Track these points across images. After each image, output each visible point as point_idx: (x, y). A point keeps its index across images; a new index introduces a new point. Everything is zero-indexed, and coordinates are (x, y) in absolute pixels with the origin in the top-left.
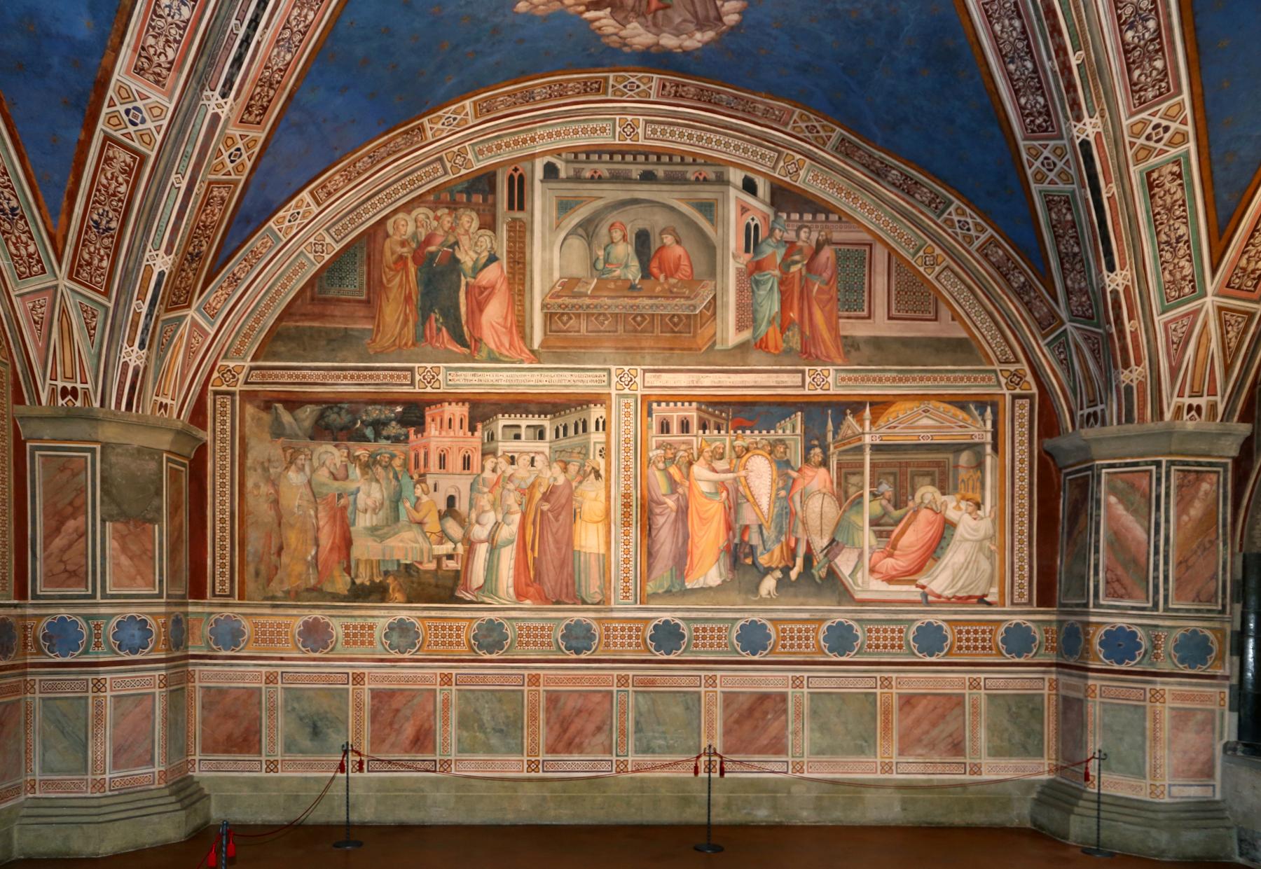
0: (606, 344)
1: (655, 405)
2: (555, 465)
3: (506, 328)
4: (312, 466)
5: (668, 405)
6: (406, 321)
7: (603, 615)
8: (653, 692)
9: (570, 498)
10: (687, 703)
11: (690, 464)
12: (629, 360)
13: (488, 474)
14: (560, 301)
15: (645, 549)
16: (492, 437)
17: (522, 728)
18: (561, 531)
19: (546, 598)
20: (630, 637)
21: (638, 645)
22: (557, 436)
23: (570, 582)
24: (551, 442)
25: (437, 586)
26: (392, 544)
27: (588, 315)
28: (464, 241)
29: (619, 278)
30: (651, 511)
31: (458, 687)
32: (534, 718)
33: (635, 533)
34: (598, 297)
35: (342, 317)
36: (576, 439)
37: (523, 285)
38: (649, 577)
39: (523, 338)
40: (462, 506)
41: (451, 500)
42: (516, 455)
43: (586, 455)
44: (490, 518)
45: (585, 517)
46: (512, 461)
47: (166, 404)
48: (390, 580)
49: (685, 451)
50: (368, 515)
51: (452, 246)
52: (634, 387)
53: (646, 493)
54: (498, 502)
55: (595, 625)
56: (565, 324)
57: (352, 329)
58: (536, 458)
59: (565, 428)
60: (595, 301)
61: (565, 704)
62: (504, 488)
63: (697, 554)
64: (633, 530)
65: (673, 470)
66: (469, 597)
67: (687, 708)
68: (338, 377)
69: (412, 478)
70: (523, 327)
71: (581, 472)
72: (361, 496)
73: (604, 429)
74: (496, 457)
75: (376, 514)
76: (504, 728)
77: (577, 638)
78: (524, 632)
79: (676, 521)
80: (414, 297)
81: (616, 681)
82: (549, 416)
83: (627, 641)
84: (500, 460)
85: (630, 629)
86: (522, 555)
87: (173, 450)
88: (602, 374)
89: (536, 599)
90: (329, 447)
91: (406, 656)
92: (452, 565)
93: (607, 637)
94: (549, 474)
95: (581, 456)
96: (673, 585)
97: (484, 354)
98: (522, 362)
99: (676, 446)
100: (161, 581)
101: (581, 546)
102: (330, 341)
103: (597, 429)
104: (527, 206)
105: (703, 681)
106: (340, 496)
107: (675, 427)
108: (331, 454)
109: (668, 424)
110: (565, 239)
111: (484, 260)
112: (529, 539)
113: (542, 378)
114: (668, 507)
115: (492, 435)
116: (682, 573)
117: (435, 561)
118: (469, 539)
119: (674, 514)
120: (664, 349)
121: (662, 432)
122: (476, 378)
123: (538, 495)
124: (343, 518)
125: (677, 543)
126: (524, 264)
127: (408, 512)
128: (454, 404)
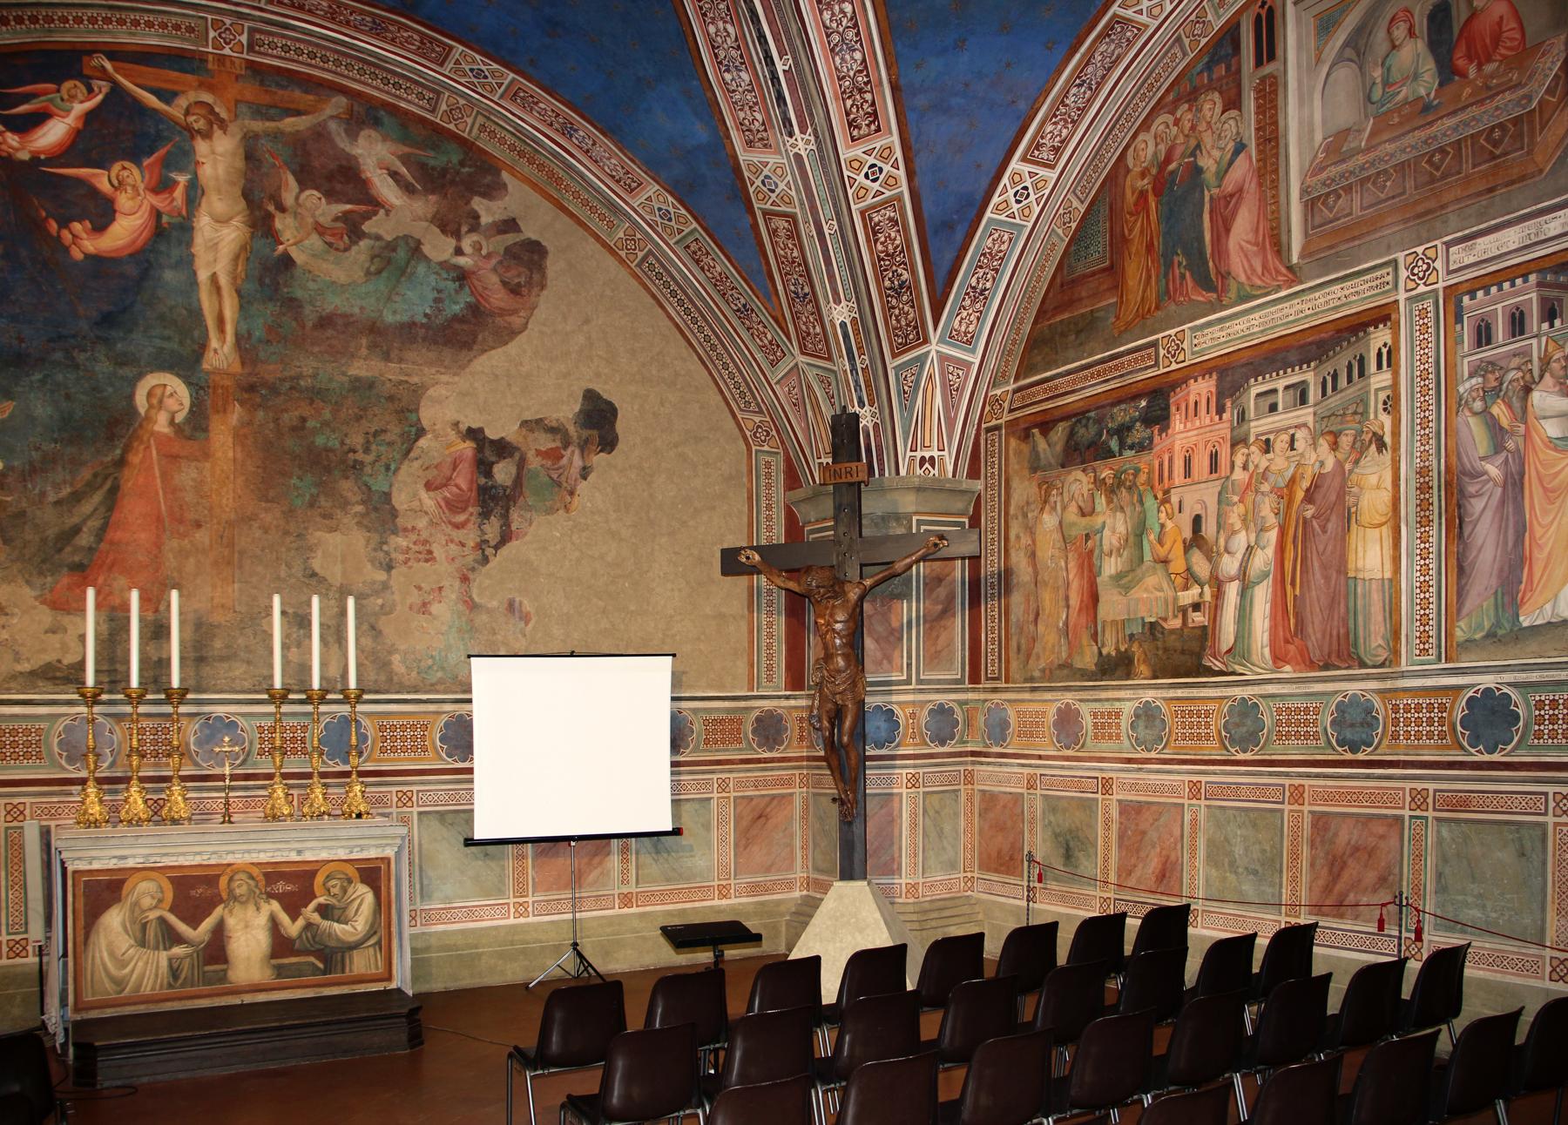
0: (1389, 220)
1: (1466, 299)
2: (1321, 441)
3: (1256, 244)
4: (1062, 500)
5: (1487, 293)
6: (1149, 277)
7: (1388, 684)
8: (1467, 821)
9: (1342, 493)
10: (1522, 846)
11: (1528, 390)
12: (1424, 235)
13: (1239, 475)
14: (1324, 175)
15: (1453, 562)
16: (1242, 417)
17: (1281, 871)
18: (1330, 548)
19: (1312, 662)
20: (1430, 722)
21: (1442, 735)
22: (1324, 394)
23: (1342, 631)
24: (1315, 405)
25: (1183, 652)
26: (1137, 596)
27: (1363, 181)
28: (1208, 139)
29: (1406, 102)
30: (1461, 492)
31: (1208, 803)
32: (1295, 856)
33: (1437, 534)
34: (1375, 147)
35: (1088, 297)
36: (1351, 390)
37: (1276, 171)
38: (1459, 610)
39: (1278, 253)
40: (1209, 529)
41: (1197, 520)
42: (1272, 437)
43: (1365, 414)
44: (1241, 541)
45: (1365, 518)
46: (1267, 447)
47: (932, 458)
48: (1135, 648)
49: (1519, 369)
50: (1113, 559)
51: (1193, 154)
52: (1432, 279)
53: (1454, 459)
54: (1250, 517)
55: (1377, 703)
56: (1331, 210)
57: (1098, 310)
58: (1297, 436)
59: (1335, 377)
60: (1371, 156)
61: (1336, 835)
62: (1257, 492)
63: (1540, 557)
64: (1434, 532)
65: (1499, 410)
66: (1218, 666)
67: (1522, 854)
68: (1086, 378)
69: (1156, 498)
70: (1278, 235)
71: (1358, 444)
72: (1106, 532)
73: (1389, 365)
74: (1247, 446)
75: (1121, 556)
76: (1258, 868)
77: (1352, 725)
78: (1284, 717)
79: (1502, 502)
80: (1156, 243)
81: (1408, 799)
82: (1312, 364)
83: (1425, 728)
84: (1253, 448)
85: (1430, 708)
86: (1279, 594)
87: (921, 509)
88: (1384, 271)
89: (1298, 664)
90: (1078, 474)
91: (1153, 755)
92: (1198, 618)
93: (1396, 722)
94: (1314, 456)
95: (1358, 417)
96: (1498, 624)
97: (1232, 294)
98: (1278, 288)
99: (1502, 364)
100: (909, 665)
101: (1357, 570)
102: (1078, 332)
103: (1379, 366)
104: (1279, 52)
105: (1552, 804)
106: (1088, 537)
107: (1500, 330)
108: (1078, 482)
109: (1488, 327)
110: (1328, 75)
111: (1229, 156)
112: (1288, 566)
113: (1305, 306)
114: (1491, 479)
115: (1243, 412)
116: (1514, 599)
117: (1180, 616)
118: (1217, 578)
119: (1499, 490)
120: (1480, 194)
121: (1479, 345)
122: (1224, 333)
123: (1300, 495)
124: (1091, 566)
125: (1505, 543)
126: (1277, 138)
127: (1152, 548)
128: (1200, 379)
